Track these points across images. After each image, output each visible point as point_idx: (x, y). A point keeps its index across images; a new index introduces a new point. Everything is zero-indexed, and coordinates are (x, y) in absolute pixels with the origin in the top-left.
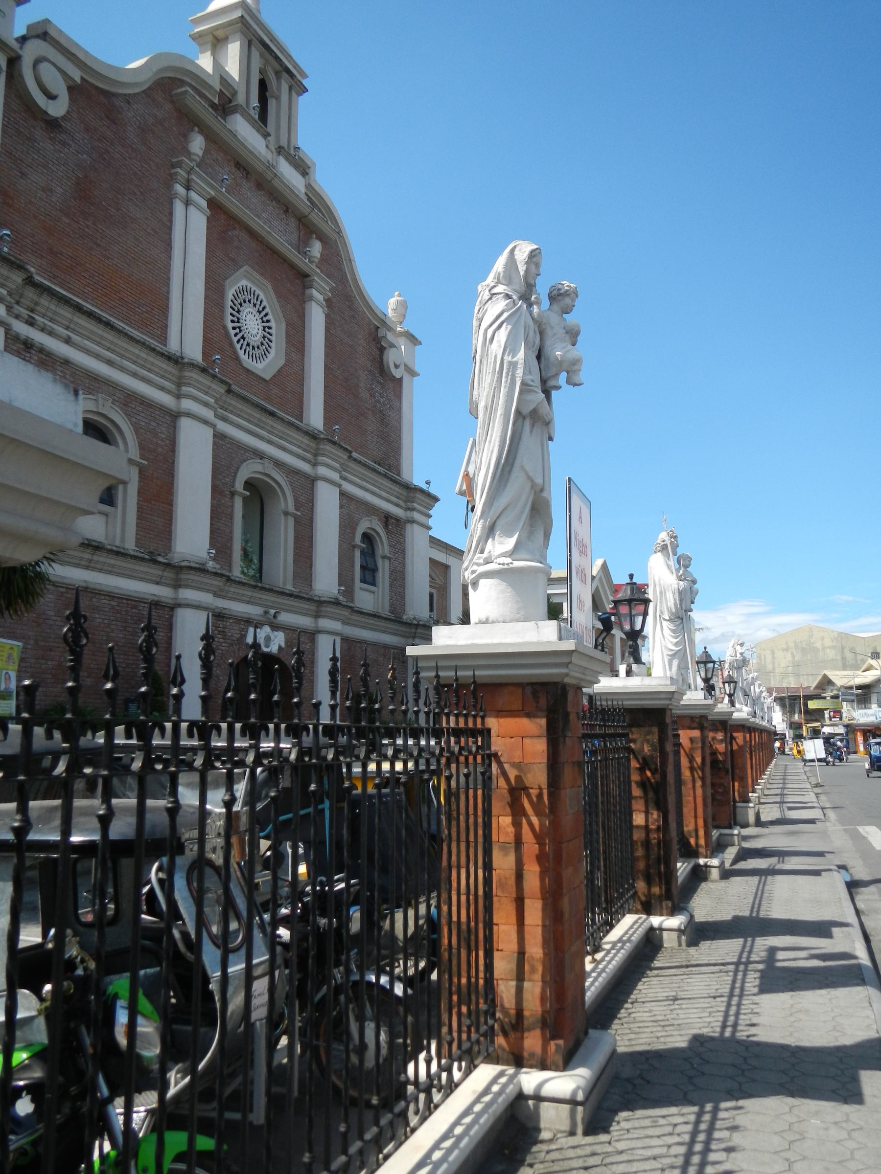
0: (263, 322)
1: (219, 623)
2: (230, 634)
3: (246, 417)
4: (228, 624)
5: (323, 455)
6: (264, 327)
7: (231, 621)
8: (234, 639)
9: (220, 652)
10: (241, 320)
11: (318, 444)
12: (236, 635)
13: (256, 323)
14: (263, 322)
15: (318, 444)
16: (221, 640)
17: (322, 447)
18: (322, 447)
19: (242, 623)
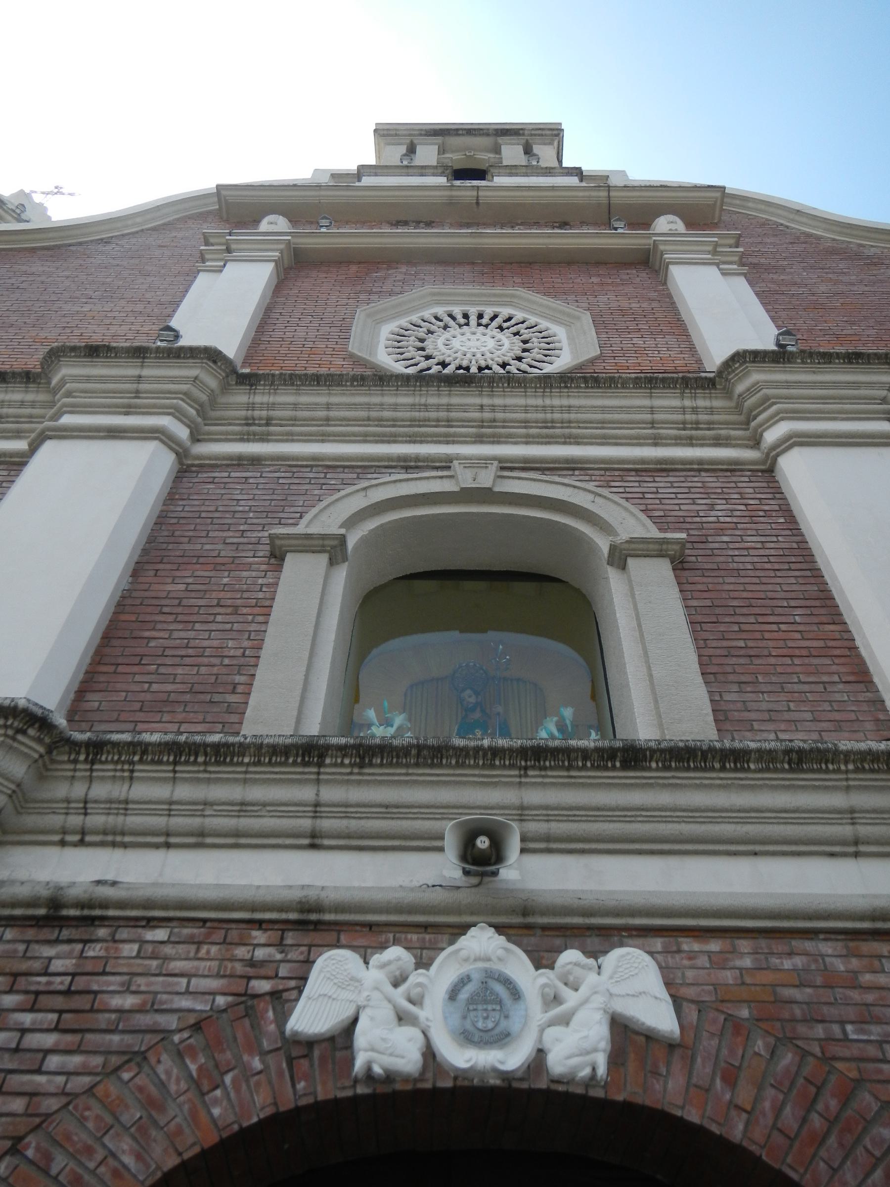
0: (487, 326)
1: (48, 951)
2: (129, 1001)
3: (363, 414)
4: (130, 949)
5: (766, 402)
6: (479, 325)
7: (161, 934)
8: (171, 1022)
9: (18, 1105)
10: (447, 360)
11: (728, 393)
12: (185, 1003)
13: (478, 335)
14: (487, 326)
15: (728, 393)
16: (49, 1040)
17: (740, 388)
18: (740, 388)
19: (259, 936)
